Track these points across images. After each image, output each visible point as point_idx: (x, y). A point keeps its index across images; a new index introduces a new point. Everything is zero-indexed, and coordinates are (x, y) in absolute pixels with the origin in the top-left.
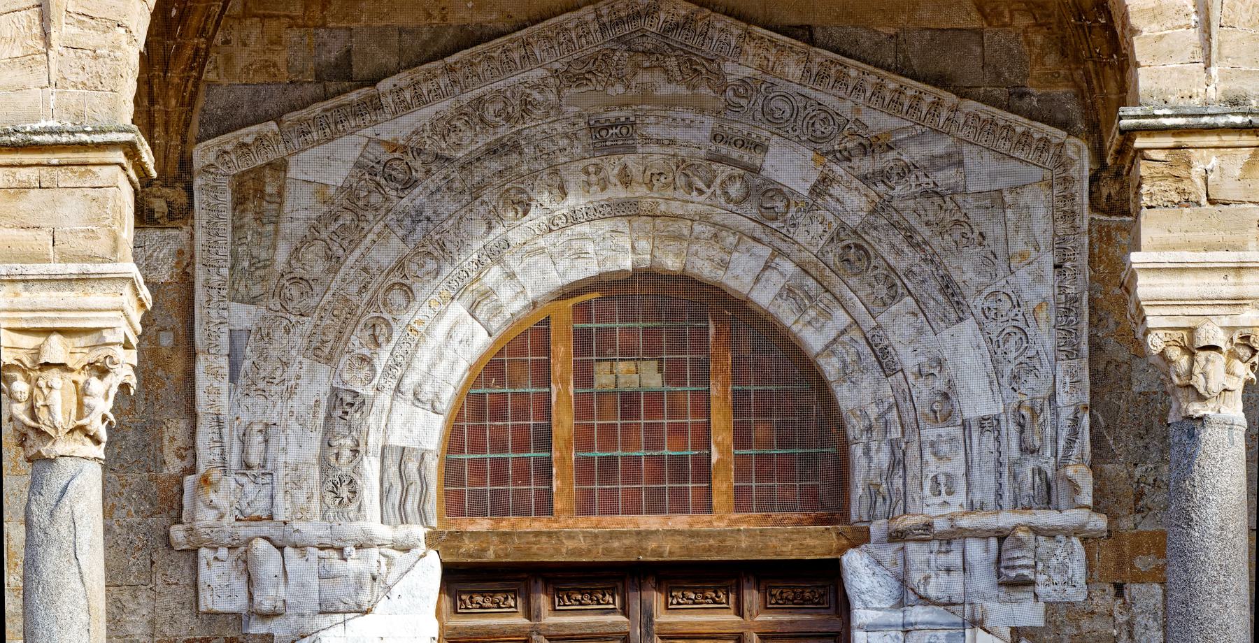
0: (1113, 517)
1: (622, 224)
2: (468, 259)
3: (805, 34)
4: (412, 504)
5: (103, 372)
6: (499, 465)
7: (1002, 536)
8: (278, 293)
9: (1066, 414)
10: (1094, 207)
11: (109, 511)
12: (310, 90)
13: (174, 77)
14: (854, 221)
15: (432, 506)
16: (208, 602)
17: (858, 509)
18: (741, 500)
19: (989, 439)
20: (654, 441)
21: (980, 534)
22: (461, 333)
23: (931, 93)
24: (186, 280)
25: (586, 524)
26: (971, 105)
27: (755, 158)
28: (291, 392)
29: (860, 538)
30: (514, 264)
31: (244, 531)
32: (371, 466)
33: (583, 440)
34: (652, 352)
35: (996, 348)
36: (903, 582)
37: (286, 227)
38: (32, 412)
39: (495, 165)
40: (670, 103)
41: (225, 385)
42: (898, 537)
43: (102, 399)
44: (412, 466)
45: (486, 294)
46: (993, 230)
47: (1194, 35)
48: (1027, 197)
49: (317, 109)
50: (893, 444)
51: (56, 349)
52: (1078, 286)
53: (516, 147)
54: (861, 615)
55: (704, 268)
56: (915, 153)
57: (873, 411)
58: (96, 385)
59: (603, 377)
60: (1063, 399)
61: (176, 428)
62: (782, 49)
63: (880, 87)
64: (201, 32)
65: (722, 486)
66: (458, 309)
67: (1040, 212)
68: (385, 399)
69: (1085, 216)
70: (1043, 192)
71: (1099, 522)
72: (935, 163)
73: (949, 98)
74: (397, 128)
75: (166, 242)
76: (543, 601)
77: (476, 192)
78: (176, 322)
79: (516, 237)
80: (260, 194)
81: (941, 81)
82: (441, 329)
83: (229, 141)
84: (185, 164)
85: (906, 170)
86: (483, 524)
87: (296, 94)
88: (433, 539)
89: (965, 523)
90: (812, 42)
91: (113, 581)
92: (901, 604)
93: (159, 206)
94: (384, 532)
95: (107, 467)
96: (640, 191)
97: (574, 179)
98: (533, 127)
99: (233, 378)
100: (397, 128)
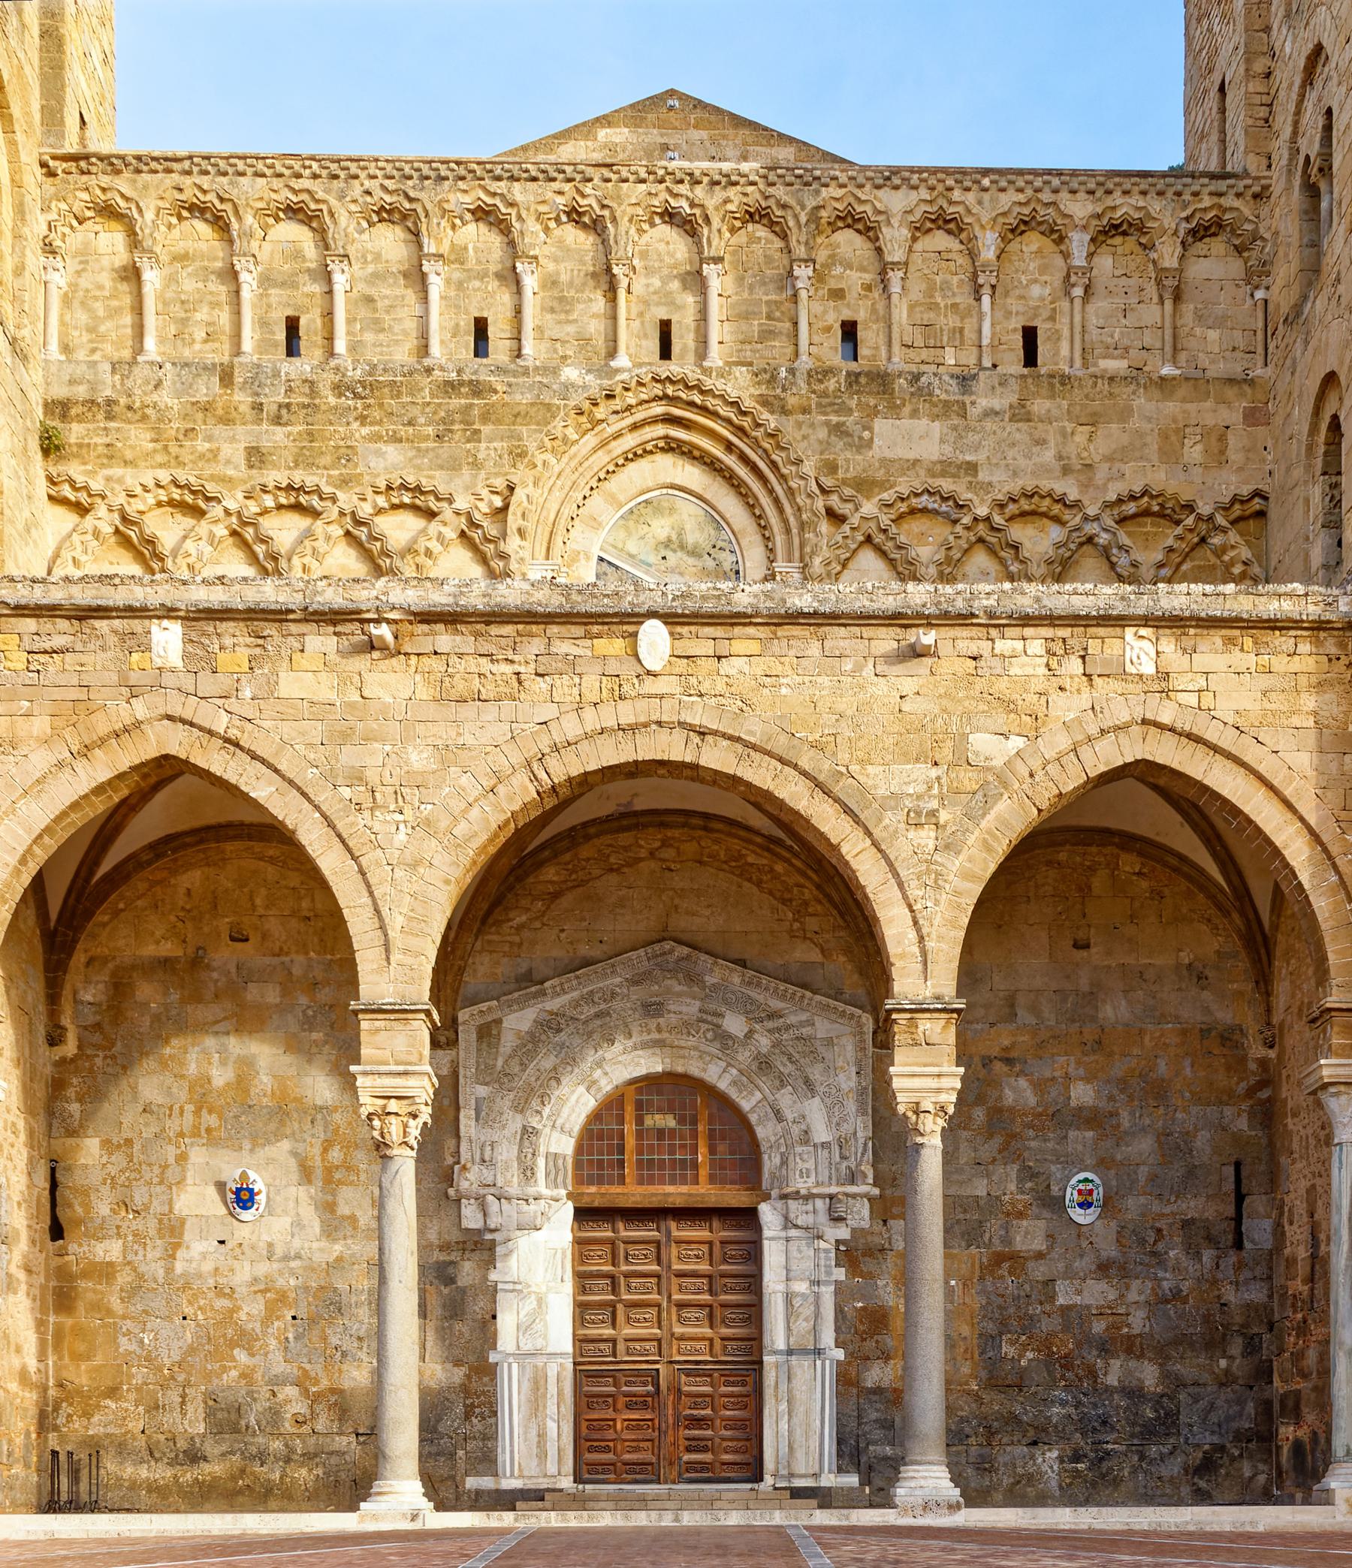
0: (882, 1189)
1: (658, 1051)
2: (585, 1067)
3: (742, 963)
4: (560, 1179)
5: (415, 1116)
6: (600, 1162)
7: (831, 1197)
8: (498, 1081)
9: (861, 1141)
10: (875, 1046)
11: (418, 1181)
12: (512, 986)
13: (449, 979)
14: (764, 1050)
15: (569, 1181)
16: (465, 1224)
17: (765, 1185)
18: (712, 1179)
19: (826, 1152)
20: (672, 1152)
21: (822, 1196)
22: (583, 1100)
23: (800, 991)
24: (455, 1074)
25: (641, 1189)
26: (818, 998)
27: (719, 1021)
28: (504, 1127)
29: (766, 1197)
30: (608, 1069)
31: (482, 1191)
32: (541, 1162)
33: (640, 1152)
34: (671, 1110)
35: (829, 1109)
36: (786, 1218)
37: (502, 1050)
38: (382, 1135)
39: (599, 1022)
40: (680, 995)
41: (473, 1123)
42: (784, 1197)
43: (415, 1129)
44: (560, 1162)
45: (594, 1082)
46: (828, 1056)
47: (920, 967)
48: (844, 1040)
49: (516, 995)
50: (782, 1154)
51: (393, 1106)
52: (867, 1082)
53: (608, 1014)
54: (767, 1233)
55: (694, 1069)
56: (792, 1019)
57: (773, 1139)
58: (412, 1123)
59: (648, 1122)
60: (860, 1134)
61: (451, 1143)
62: (731, 970)
63: (776, 989)
64: (462, 958)
65: (704, 1172)
66: (582, 1089)
67: (850, 1048)
68: (547, 1130)
69: (871, 1049)
70: (851, 1039)
71: (876, 1191)
72: (802, 1024)
73: (808, 994)
74: (554, 1004)
75: (445, 1056)
76: (620, 1225)
77: (590, 1034)
78: (450, 1093)
79: (608, 1056)
80: (490, 1035)
81: (804, 986)
82: (574, 1098)
83: (475, 1009)
84: (455, 1021)
85: (788, 1027)
86: (593, 1189)
87: (506, 988)
88: (570, 1196)
89: (815, 1191)
90: (745, 966)
91: (421, 1214)
92: (785, 1228)
93: (443, 1039)
94: (546, 1192)
95: (418, 1161)
96: (665, 1035)
97: (635, 1029)
98: (617, 1004)
99: (477, 1120)
100: (554, 1004)
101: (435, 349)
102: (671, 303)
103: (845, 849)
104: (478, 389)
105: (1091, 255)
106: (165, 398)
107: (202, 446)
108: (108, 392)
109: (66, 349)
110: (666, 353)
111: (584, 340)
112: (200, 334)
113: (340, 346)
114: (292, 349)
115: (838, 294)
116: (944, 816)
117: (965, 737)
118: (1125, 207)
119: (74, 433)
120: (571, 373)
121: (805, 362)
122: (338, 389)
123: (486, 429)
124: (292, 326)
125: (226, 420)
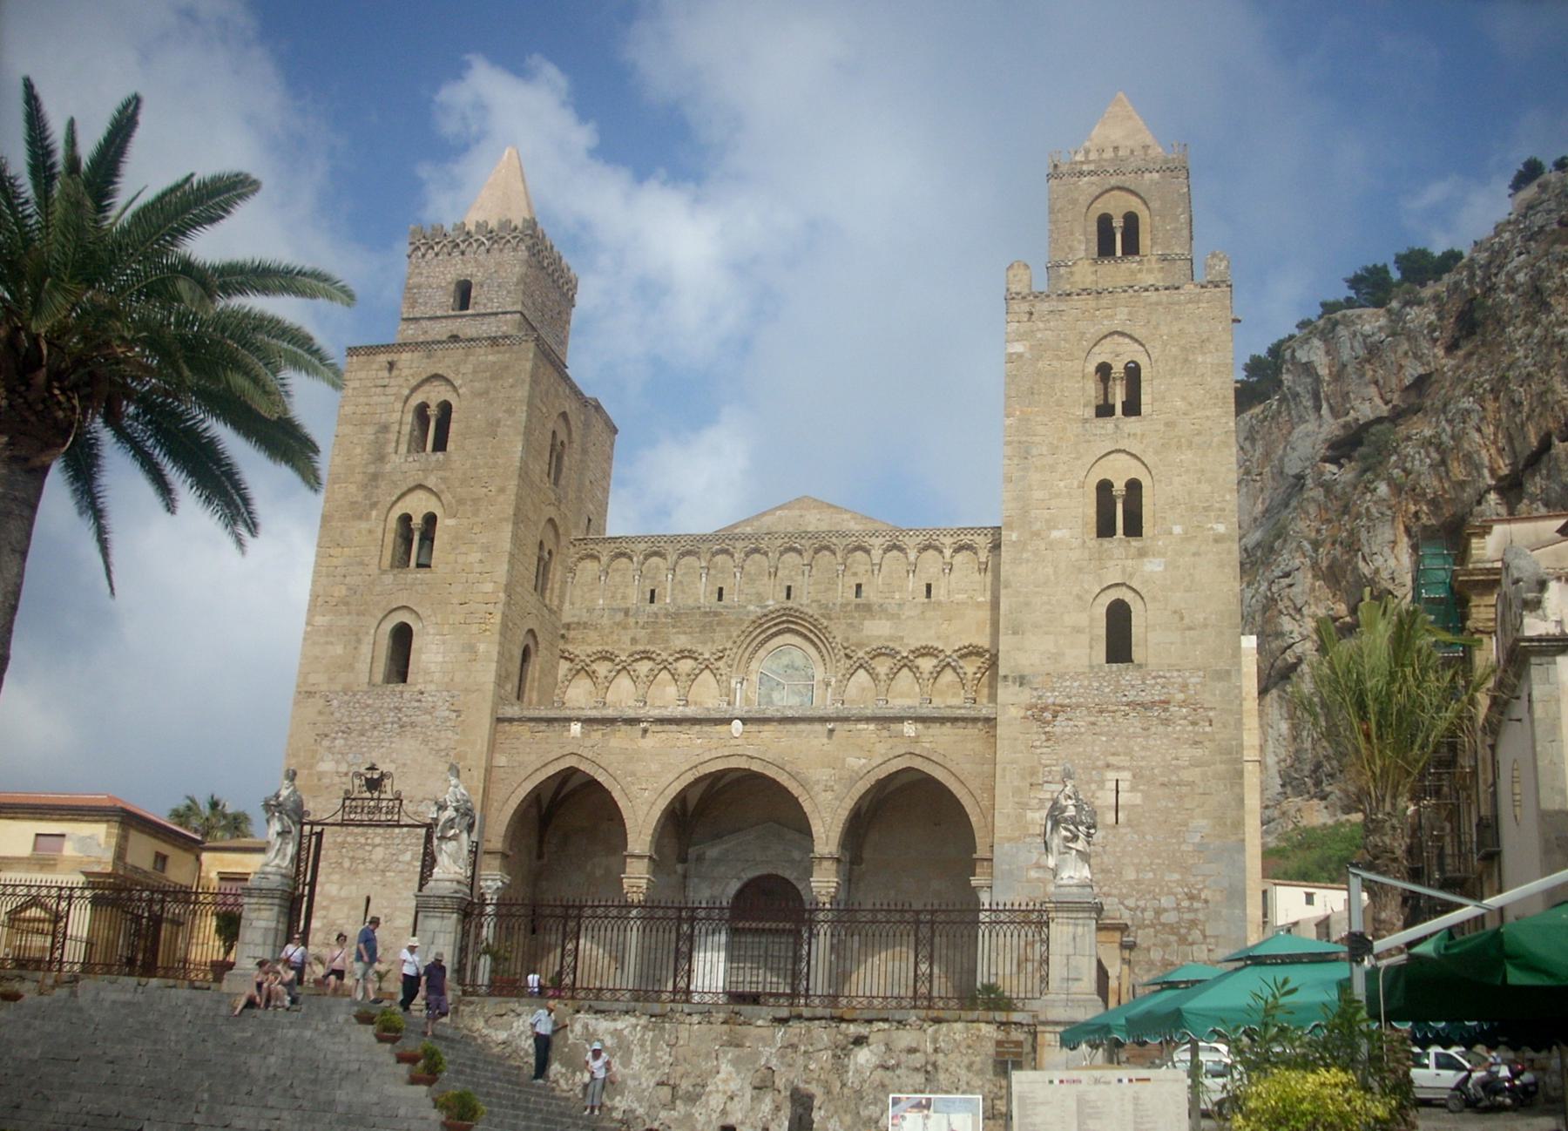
101: (702, 601)
102: (791, 579)
103: (800, 800)
104: (716, 614)
105: (952, 557)
106: (605, 621)
107: (615, 637)
108: (584, 619)
109: (572, 604)
110: (788, 596)
111: (759, 594)
112: (619, 596)
113: (668, 601)
114: (652, 601)
115: (855, 574)
116: (836, 787)
117: (844, 759)
118: (966, 539)
119: (572, 634)
120: (751, 608)
121: (839, 601)
122: (666, 616)
123: (718, 629)
124: (653, 592)
125: (625, 628)
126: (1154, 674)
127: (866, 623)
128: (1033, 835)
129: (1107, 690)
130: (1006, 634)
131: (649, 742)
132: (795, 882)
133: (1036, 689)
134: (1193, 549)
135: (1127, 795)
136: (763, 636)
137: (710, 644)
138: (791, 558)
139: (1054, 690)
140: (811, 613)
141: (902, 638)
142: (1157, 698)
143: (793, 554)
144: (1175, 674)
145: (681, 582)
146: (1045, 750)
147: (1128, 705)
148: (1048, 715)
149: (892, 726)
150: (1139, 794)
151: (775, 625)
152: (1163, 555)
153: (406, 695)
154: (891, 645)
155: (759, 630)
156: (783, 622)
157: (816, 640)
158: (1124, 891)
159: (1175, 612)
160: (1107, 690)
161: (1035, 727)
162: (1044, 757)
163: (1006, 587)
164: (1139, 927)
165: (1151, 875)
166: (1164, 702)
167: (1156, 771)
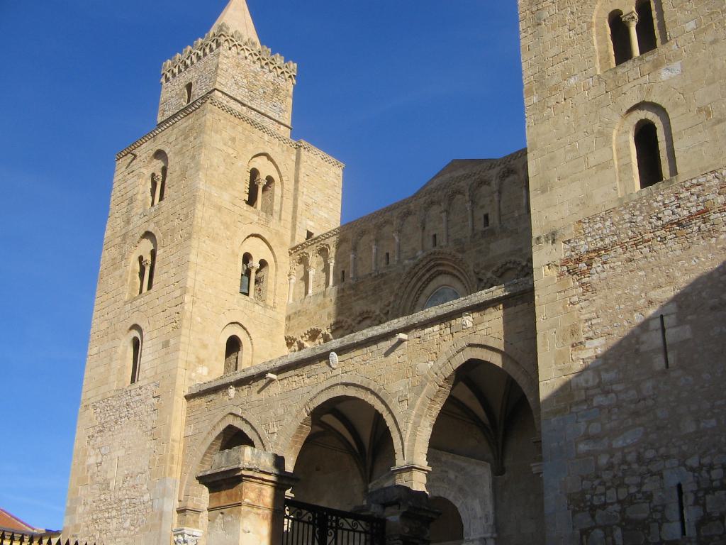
104: (382, 275)
108: (299, 309)
110: (435, 244)
124: (343, 272)
125: (324, 308)
126: (688, 184)
127: (492, 246)
128: (577, 404)
129: (640, 218)
130: (537, 195)
131: (275, 389)
132: (453, 502)
133: (569, 241)
134: (709, 38)
135: (674, 330)
136: (420, 284)
137: (379, 303)
138: (435, 210)
139: (586, 237)
140: (448, 251)
141: (521, 250)
142: (694, 210)
143: (435, 207)
144: (710, 177)
145: (361, 258)
146: (583, 304)
147: (663, 227)
148: (583, 266)
149: (453, 322)
150: (688, 327)
151: (428, 271)
152: (677, 57)
153: (133, 393)
154: (513, 259)
155: (415, 279)
156: (433, 267)
157: (458, 274)
158: (685, 448)
159: (700, 110)
160: (640, 218)
161: (572, 281)
162: (583, 311)
163: (532, 150)
164: (707, 491)
165: (713, 422)
166: (699, 213)
167: (704, 294)
